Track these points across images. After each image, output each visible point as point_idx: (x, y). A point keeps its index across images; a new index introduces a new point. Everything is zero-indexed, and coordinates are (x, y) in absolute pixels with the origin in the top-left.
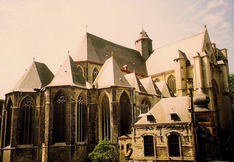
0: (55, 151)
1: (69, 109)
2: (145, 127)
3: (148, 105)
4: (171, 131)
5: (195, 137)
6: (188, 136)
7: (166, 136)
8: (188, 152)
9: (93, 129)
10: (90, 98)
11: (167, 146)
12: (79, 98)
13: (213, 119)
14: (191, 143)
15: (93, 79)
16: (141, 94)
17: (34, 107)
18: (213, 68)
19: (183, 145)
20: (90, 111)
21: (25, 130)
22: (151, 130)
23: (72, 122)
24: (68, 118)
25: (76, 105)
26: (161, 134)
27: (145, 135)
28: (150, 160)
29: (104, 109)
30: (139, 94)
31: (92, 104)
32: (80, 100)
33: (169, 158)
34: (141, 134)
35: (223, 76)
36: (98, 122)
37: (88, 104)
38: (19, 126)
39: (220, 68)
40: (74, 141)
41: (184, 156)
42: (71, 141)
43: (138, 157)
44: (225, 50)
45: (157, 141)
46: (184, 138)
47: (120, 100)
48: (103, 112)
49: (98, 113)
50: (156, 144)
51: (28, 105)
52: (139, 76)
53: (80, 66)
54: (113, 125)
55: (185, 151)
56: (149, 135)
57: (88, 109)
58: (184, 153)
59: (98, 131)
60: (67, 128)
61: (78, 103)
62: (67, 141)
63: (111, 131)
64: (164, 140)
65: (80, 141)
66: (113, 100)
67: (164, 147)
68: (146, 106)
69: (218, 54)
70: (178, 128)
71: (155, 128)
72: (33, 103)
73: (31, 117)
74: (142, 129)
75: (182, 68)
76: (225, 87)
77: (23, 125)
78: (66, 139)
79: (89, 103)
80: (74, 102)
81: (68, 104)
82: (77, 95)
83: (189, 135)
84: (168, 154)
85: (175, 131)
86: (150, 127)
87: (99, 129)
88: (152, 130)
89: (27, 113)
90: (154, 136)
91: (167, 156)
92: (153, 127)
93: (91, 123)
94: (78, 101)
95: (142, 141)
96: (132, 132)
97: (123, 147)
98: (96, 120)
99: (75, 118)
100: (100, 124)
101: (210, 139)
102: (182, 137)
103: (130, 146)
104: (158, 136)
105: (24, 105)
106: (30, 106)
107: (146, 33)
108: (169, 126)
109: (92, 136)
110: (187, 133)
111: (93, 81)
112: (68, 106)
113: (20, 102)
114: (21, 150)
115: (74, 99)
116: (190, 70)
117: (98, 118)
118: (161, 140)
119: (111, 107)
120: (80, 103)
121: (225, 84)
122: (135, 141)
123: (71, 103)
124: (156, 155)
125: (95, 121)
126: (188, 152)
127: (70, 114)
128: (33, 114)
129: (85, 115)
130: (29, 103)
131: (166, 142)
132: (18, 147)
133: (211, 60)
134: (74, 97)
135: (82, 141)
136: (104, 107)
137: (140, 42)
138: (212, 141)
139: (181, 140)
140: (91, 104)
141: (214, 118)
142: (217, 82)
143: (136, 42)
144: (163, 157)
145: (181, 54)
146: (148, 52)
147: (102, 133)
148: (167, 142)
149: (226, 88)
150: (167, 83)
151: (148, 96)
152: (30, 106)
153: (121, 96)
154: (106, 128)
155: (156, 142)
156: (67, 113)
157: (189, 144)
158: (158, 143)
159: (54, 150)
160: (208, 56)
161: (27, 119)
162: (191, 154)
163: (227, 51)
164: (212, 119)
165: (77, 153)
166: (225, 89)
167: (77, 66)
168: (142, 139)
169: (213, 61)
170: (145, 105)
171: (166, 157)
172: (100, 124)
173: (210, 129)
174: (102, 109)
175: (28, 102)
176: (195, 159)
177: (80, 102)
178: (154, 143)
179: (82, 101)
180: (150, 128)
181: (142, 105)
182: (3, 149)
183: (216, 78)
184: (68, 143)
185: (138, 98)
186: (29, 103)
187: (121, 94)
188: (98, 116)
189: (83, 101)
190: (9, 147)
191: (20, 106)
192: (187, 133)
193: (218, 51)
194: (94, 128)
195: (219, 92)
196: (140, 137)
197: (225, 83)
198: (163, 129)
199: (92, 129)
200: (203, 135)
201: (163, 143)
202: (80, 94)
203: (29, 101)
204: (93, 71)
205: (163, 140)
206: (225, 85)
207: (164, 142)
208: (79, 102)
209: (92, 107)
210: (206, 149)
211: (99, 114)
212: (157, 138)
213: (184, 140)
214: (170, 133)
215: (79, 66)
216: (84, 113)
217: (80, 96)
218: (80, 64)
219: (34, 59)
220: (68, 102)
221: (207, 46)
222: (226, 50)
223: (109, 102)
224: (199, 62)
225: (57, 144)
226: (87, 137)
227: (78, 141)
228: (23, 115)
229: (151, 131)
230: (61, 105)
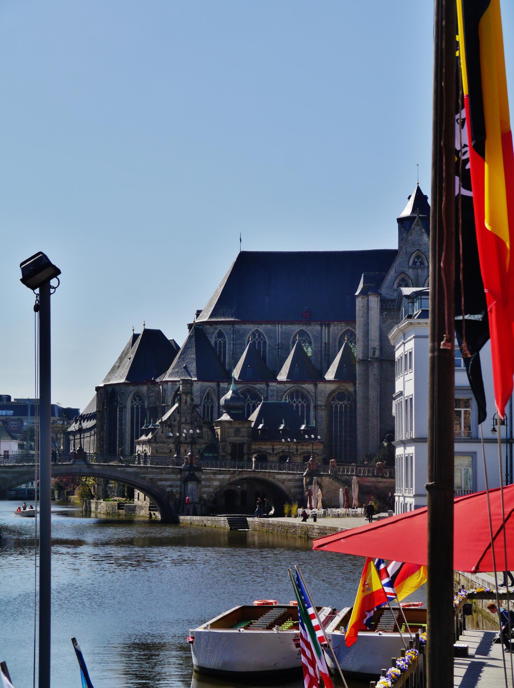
13: (223, 432)
31: (151, 406)
52: (340, 325)
61: (133, 406)
82: (129, 396)
99: (123, 427)
120: (137, 406)
134: (122, 399)
141: (225, 430)
151: (255, 384)
204: (216, 338)
208: (135, 404)
219: (133, 330)
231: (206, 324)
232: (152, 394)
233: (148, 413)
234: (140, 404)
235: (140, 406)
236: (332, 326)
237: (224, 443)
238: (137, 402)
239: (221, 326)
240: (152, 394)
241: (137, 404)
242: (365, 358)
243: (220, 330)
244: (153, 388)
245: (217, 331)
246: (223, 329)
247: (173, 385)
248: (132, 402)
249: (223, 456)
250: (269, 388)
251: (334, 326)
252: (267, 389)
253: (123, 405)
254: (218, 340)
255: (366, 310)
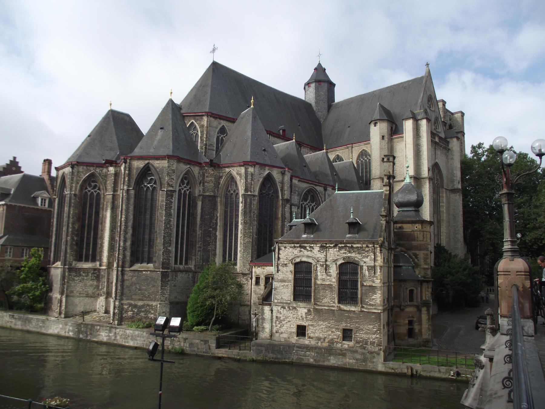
0: (134, 279)
1: (162, 201)
2: (298, 245)
3: (315, 203)
4: (345, 255)
5: (389, 267)
6: (374, 267)
7: (336, 264)
8: (373, 297)
9: (206, 243)
10: (204, 183)
11: (336, 284)
12: (182, 182)
13: (425, 236)
14: (380, 281)
15: (216, 148)
16: (301, 181)
17: (104, 194)
18: (436, 143)
19: (365, 284)
20: (202, 209)
21: (86, 235)
22: (310, 252)
23: (166, 227)
24: (160, 218)
25: (176, 195)
26: (326, 261)
27: (298, 260)
28: (302, 308)
29: (229, 205)
30: (299, 181)
31: (207, 194)
32: (184, 186)
33: (338, 306)
34: (290, 258)
35: (452, 159)
36: (215, 229)
37: (200, 195)
38: (76, 227)
39: (448, 142)
40: (169, 264)
41: (366, 304)
42: (163, 263)
43: (282, 301)
44: (460, 114)
45: (319, 273)
46: (368, 270)
47: (261, 190)
48: (226, 212)
49: (217, 213)
50: (316, 279)
51: (92, 191)
53: (194, 121)
54: (244, 238)
55: (366, 294)
56: (305, 262)
57: (199, 204)
58: (364, 297)
59: (216, 248)
60: (156, 238)
61: (180, 190)
62: (155, 262)
63: (239, 249)
64: (331, 271)
65: (181, 263)
66: (246, 190)
67: (330, 286)
68: (311, 205)
69: (448, 119)
70: (359, 250)
71: (317, 248)
72: (101, 187)
73: (97, 213)
74: (292, 248)
75: (383, 137)
76: (455, 178)
77: (82, 227)
78: (154, 259)
79: (201, 193)
80: (171, 189)
81: (161, 191)
82: (179, 177)
83: (377, 264)
84: (336, 299)
85: (353, 255)
86: (308, 245)
87: (218, 243)
88: (311, 251)
89: (91, 205)
90: (314, 263)
91: (334, 303)
92: (312, 245)
93: (202, 230)
94: (180, 188)
95: (291, 272)
96: (273, 253)
97: (258, 279)
98: (213, 225)
99: (172, 220)
100: (219, 234)
101: (417, 272)
102: (365, 268)
103: (271, 278)
104: (321, 263)
105: (86, 188)
106: (95, 191)
107: (325, 69)
108: (343, 245)
109: (203, 255)
110: (375, 260)
111: (216, 152)
112: (160, 196)
113: (78, 183)
114: (78, 271)
115: (172, 183)
116: (398, 142)
117: (216, 224)
118: (326, 269)
119: (242, 203)
120: (185, 191)
121: (454, 174)
122: (278, 271)
123: (165, 190)
124: (314, 299)
125: (211, 227)
126: (373, 297)
127: (162, 211)
128: (101, 206)
129: (192, 215)
130: (95, 186)
131: (335, 275)
132: (73, 265)
133: (433, 127)
135: (184, 264)
136: (229, 202)
137: (313, 85)
138: (420, 276)
139: (362, 273)
140: (205, 194)
141: (426, 234)
142: (441, 167)
143: (305, 85)
144: (326, 304)
145: (383, 112)
146: (326, 107)
147: (223, 250)
148: (337, 276)
149: (456, 182)
150: (355, 165)
151: (316, 185)
152: (96, 191)
153: (263, 185)
154: (231, 242)
155: (317, 275)
156: (158, 209)
157: (377, 281)
158: (319, 277)
159: (133, 276)
160: (429, 120)
161: (90, 217)
162: (378, 301)
163: (464, 117)
164: (423, 236)
165: (173, 285)
166: (455, 183)
167: (190, 121)
168: (291, 267)
169: (438, 130)
170: (309, 203)
171: (332, 305)
172: (219, 234)
173: (418, 255)
174: (225, 206)
175: (93, 184)
176: (384, 310)
177: (185, 189)
178: (313, 276)
179: (189, 187)
180: (308, 248)
181: (303, 203)
182: (50, 266)
183: (441, 160)
184: (157, 265)
185: (297, 190)
186: (95, 186)
187: (262, 179)
188: (217, 218)
189: (190, 188)
190: (58, 264)
191: (79, 190)
192: (375, 260)
193: (450, 114)
194: (208, 240)
195: (445, 187)
196: (287, 263)
197: (455, 172)
198: (331, 251)
199: (203, 243)
200: (405, 266)
201: (329, 278)
202: (185, 174)
203: (94, 182)
204: (218, 133)
205: (330, 272)
206: (455, 175)
207: (330, 276)
208: (183, 189)
209: (207, 200)
210: (408, 291)
211: (218, 215)
212: (319, 269)
213: (367, 273)
214: (344, 259)
215: (192, 123)
216: (191, 211)
217: (184, 178)
218: (194, 119)
220: (161, 188)
221: (429, 101)
222: (463, 114)
223: (238, 194)
224: (413, 129)
225: (137, 267)
226: (193, 257)
227: (176, 263)
228: (84, 208)
229: (309, 253)
230: (149, 194)
231: (211, 116)
232: (210, 178)
233: (199, 204)
234: (188, 190)
235: (188, 192)
236: (302, 147)
237: (425, 252)
238: (185, 187)
239: (225, 122)
240: (210, 178)
241: (185, 189)
242: (417, 176)
243: (223, 126)
244: (213, 171)
245: (220, 127)
246: (227, 126)
247: (261, 169)
248: (180, 186)
249: (425, 269)
250: (327, 193)
251: (303, 148)
252: (325, 193)
253: (173, 187)
254: (220, 136)
255: (416, 132)
